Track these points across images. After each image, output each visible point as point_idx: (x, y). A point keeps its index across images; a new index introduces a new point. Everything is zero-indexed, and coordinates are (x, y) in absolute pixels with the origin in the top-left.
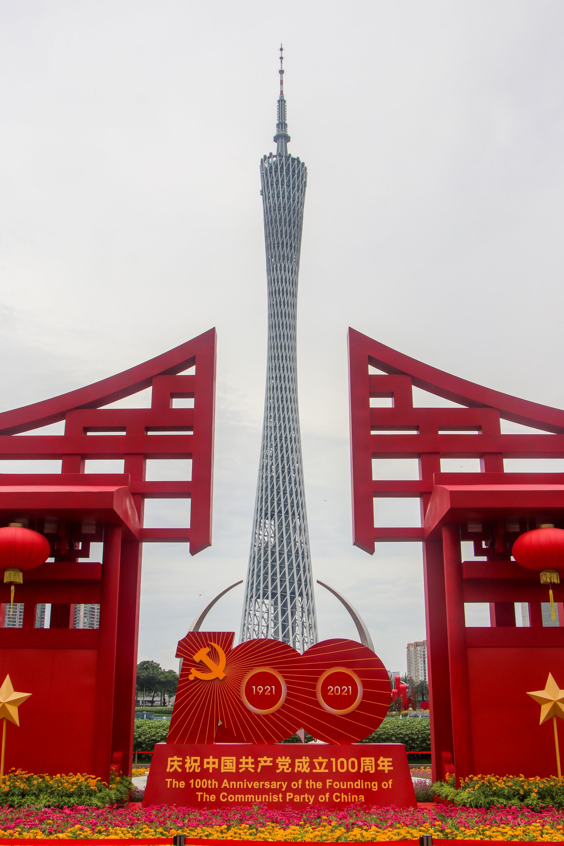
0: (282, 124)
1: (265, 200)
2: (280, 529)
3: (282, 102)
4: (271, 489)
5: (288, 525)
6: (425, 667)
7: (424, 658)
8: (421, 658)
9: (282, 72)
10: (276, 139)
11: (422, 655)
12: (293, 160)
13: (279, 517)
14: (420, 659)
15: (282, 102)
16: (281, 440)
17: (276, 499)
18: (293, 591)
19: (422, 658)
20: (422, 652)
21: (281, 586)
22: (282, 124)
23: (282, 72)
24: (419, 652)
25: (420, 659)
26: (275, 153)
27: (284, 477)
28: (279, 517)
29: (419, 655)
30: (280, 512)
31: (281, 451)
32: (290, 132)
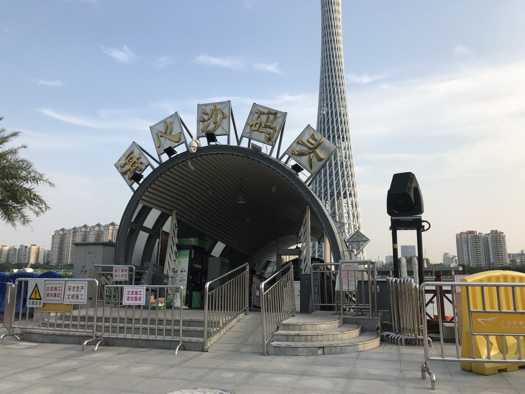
4: (327, 121)
6: (468, 249)
7: (467, 243)
8: (465, 243)
11: (466, 241)
14: (464, 244)
16: (329, 85)
17: (331, 128)
18: (339, 192)
19: (466, 243)
20: (466, 239)
21: (330, 189)
24: (464, 239)
25: (464, 244)
27: (336, 111)
29: (464, 241)
31: (330, 93)
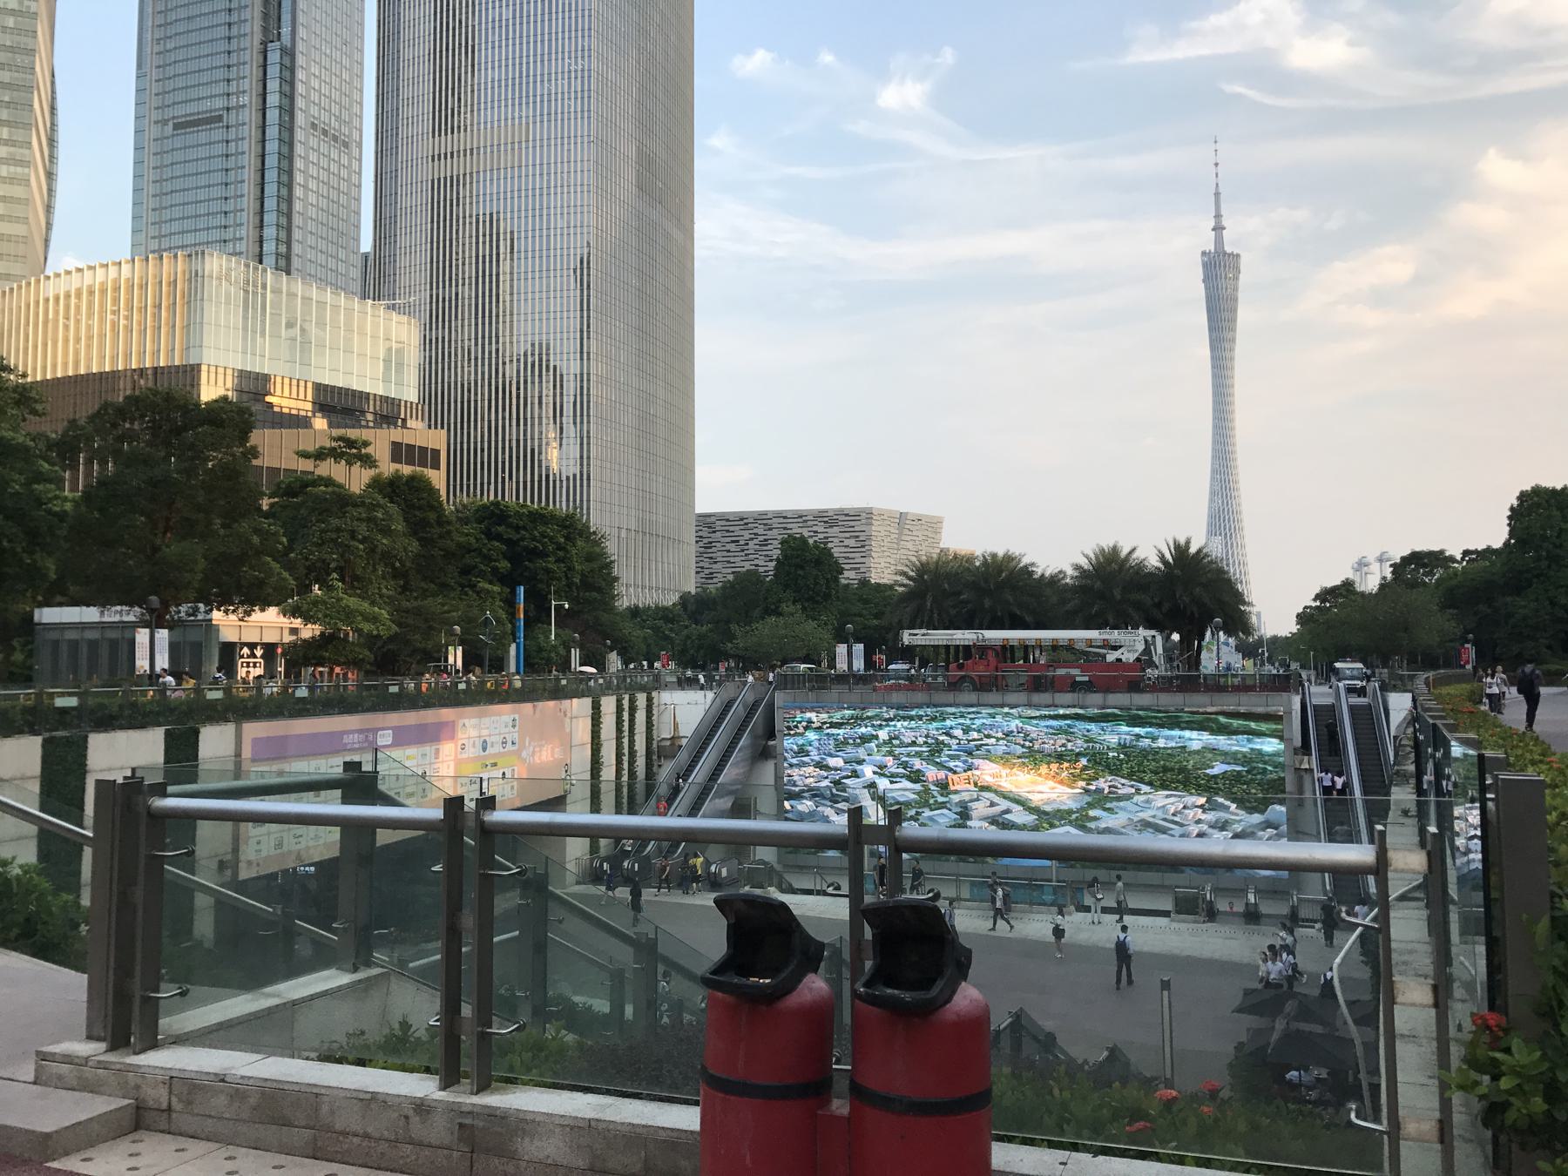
0: (1218, 216)
1: (1206, 288)
2: (1226, 546)
3: (1217, 195)
5: (1232, 544)
9: (1216, 164)
10: (1213, 230)
12: (1229, 255)
13: (1226, 538)
15: (1217, 195)
22: (1218, 216)
23: (1216, 164)
26: (1213, 251)
28: (1226, 538)
30: (1226, 534)
32: (1225, 223)
